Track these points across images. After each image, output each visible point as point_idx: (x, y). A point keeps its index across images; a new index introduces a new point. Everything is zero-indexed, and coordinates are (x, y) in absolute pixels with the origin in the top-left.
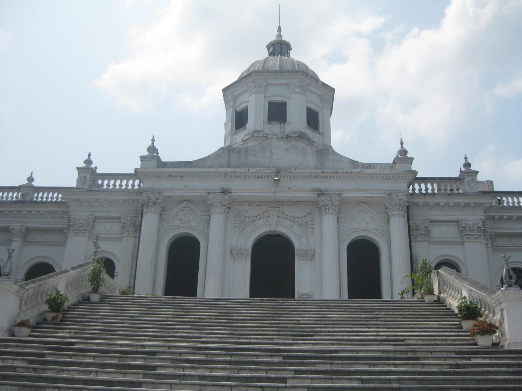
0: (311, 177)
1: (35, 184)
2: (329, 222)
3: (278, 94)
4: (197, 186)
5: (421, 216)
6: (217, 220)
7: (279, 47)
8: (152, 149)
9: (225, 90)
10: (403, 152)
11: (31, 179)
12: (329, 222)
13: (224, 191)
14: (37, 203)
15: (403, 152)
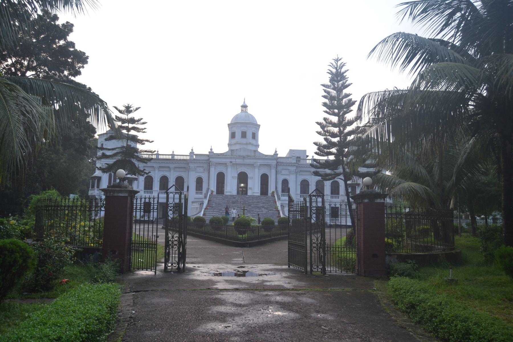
0: (253, 159)
1: (175, 153)
2: (257, 170)
3: (244, 129)
4: (223, 161)
5: (280, 168)
6: (229, 170)
7: (244, 106)
8: (211, 149)
9: (228, 124)
10: (276, 152)
11: (173, 152)
12: (257, 170)
13: (231, 162)
14: (177, 160)
15: (276, 152)
